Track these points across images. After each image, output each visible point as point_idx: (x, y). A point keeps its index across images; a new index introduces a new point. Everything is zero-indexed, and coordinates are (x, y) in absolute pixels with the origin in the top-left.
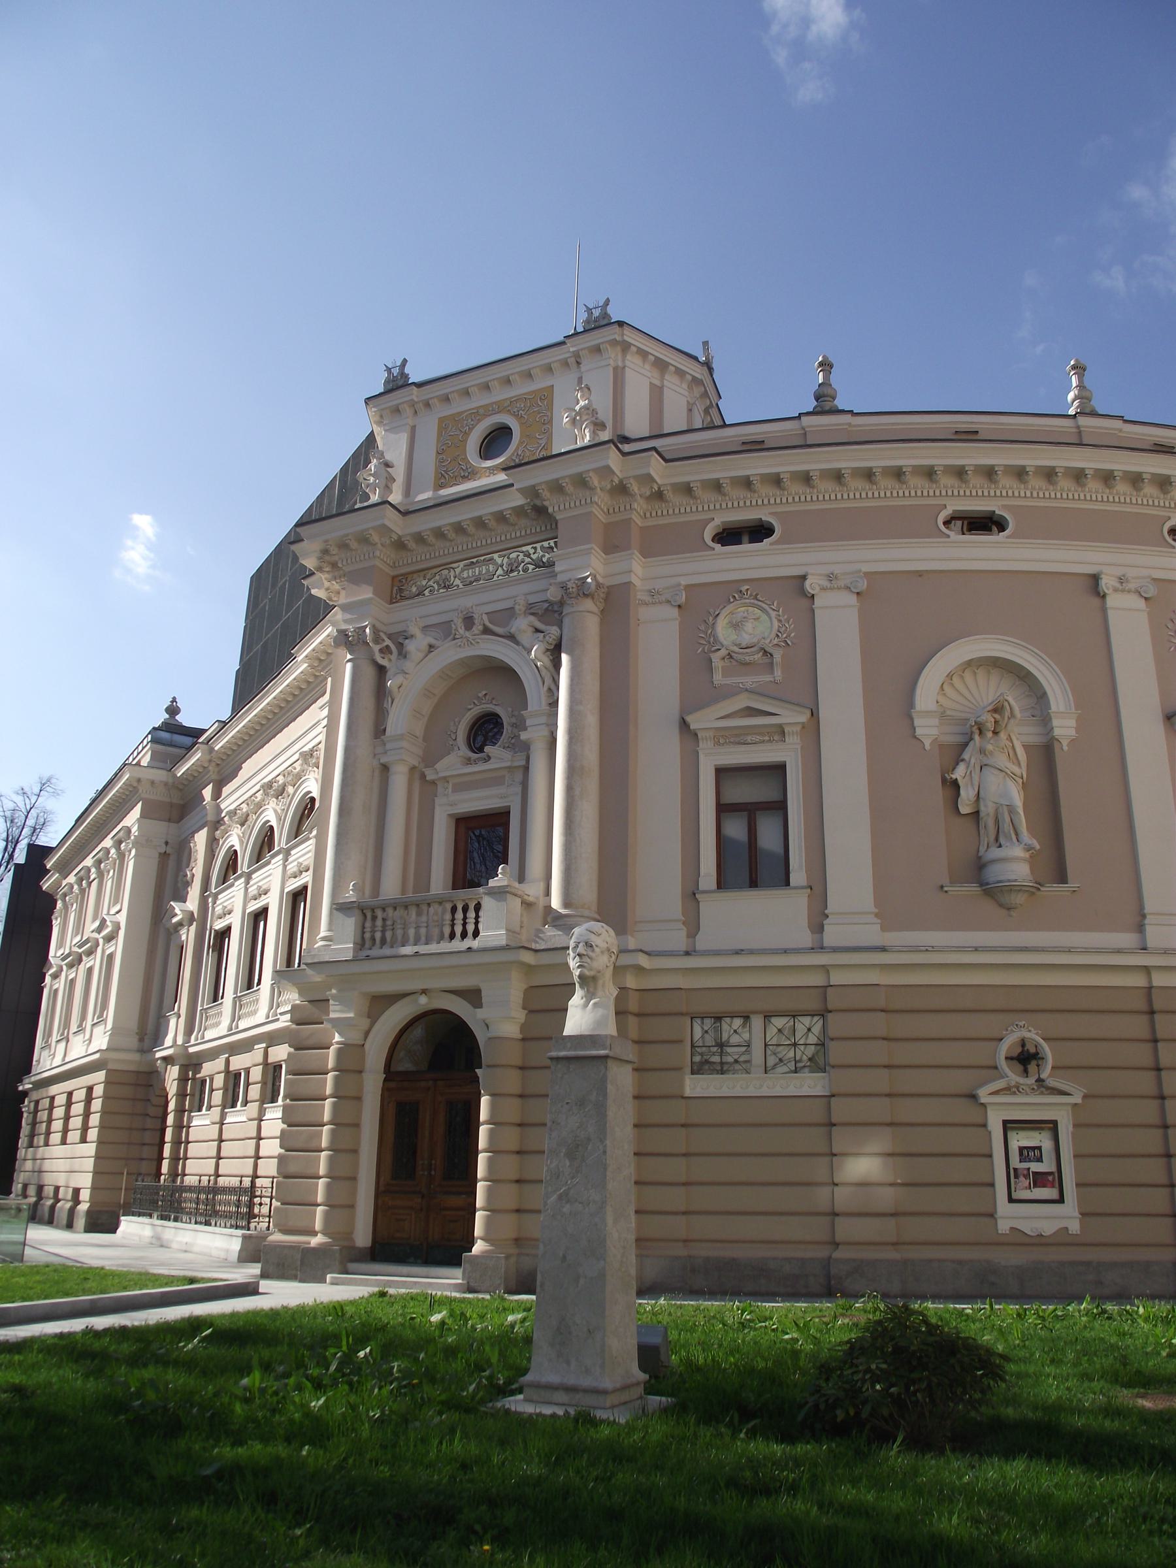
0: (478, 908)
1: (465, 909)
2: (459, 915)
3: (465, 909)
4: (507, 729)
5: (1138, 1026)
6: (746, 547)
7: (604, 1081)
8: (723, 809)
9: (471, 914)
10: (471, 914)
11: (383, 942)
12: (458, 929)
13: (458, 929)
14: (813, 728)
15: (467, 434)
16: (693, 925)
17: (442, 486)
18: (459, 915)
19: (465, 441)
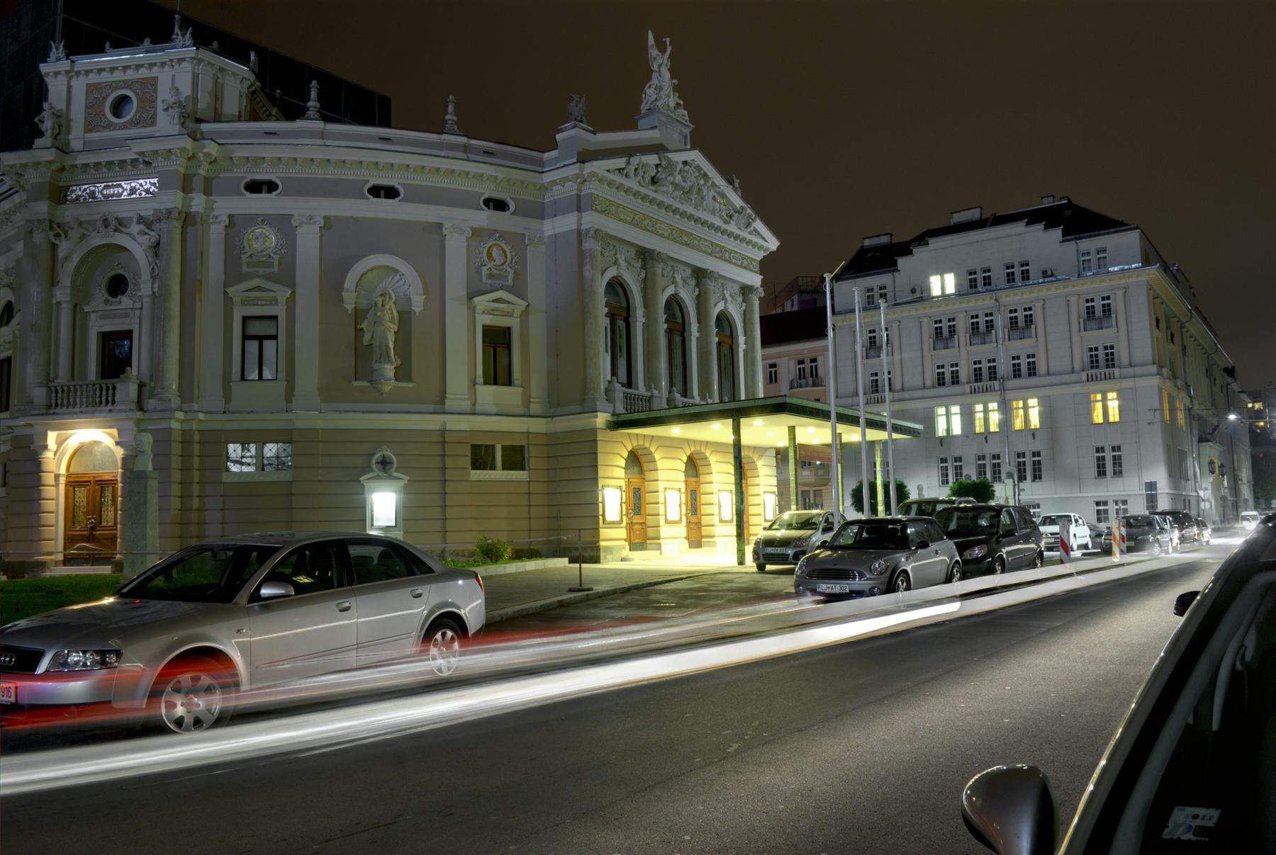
0: (114, 388)
1: (108, 389)
2: (104, 392)
3: (108, 389)
4: (131, 286)
5: (437, 450)
6: (264, 195)
7: (145, 487)
8: (246, 337)
9: (110, 392)
10: (110, 392)
11: (62, 405)
12: (104, 399)
13: (104, 399)
14: (291, 301)
15: (105, 98)
16: (227, 397)
17: (90, 131)
18: (104, 392)
19: (103, 103)
